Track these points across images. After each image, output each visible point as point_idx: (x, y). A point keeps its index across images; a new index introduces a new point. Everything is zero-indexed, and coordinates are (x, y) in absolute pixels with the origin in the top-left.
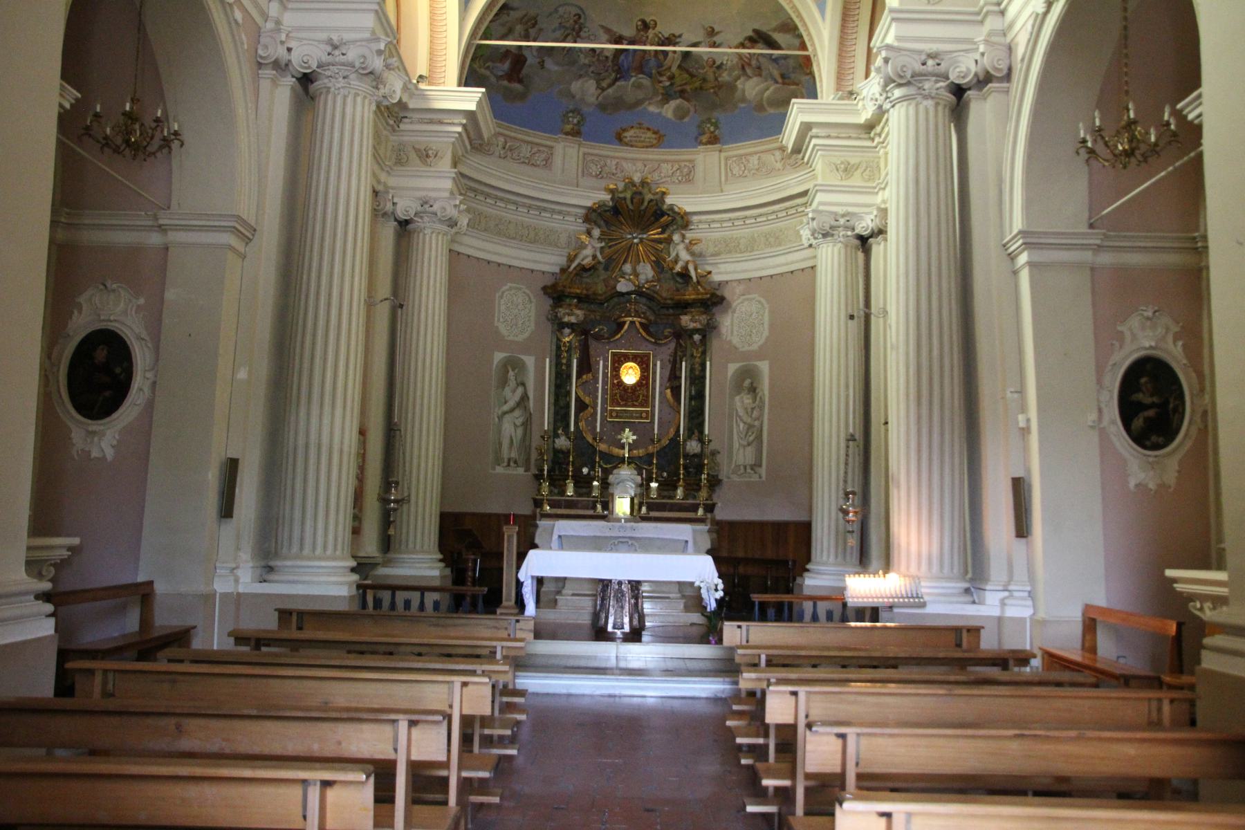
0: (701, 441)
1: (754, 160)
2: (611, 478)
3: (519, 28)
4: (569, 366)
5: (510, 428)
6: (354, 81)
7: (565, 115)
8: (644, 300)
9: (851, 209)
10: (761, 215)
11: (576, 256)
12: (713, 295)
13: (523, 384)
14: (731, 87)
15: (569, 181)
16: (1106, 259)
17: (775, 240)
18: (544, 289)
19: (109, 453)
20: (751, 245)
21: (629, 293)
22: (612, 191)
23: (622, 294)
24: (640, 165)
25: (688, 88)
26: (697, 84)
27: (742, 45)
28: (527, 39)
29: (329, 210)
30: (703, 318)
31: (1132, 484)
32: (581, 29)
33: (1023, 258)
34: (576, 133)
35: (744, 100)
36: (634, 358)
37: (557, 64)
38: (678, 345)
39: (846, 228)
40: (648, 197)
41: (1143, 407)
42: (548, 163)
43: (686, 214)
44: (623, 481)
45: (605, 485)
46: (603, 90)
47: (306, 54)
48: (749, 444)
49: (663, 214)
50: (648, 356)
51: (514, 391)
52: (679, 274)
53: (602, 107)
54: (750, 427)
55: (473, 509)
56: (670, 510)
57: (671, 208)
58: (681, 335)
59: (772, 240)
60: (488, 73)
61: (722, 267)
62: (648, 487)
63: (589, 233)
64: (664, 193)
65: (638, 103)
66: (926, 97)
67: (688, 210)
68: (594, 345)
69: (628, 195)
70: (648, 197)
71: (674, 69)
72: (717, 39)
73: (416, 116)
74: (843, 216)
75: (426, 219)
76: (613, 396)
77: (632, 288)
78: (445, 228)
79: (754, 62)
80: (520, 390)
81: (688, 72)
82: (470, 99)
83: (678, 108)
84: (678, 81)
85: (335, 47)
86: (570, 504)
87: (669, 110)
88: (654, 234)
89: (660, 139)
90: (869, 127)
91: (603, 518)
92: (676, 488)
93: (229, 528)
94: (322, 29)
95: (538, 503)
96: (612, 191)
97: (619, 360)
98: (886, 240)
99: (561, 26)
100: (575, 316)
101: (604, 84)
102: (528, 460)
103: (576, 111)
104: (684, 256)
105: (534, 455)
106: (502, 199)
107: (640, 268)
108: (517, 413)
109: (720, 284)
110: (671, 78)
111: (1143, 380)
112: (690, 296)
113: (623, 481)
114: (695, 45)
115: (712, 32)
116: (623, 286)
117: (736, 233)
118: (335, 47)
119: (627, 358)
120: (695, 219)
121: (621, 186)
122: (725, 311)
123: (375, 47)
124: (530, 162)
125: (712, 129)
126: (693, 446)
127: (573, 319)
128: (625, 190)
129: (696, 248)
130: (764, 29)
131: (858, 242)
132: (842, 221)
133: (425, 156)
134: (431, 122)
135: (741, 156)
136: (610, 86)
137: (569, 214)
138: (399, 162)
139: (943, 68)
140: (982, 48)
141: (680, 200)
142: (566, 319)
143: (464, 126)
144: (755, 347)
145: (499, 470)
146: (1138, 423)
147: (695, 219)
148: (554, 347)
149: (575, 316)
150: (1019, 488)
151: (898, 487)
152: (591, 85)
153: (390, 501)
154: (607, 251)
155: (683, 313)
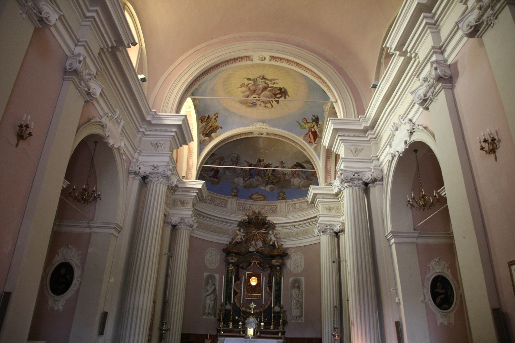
0: (280, 306)
1: (298, 205)
2: (246, 321)
3: (217, 161)
4: (232, 278)
5: (209, 301)
6: (161, 179)
7: (232, 190)
8: (259, 254)
9: (332, 223)
10: (300, 224)
11: (235, 238)
12: (284, 253)
13: (214, 285)
14: (289, 181)
15: (233, 212)
16: (420, 241)
17: (305, 233)
18: (223, 250)
19: (61, 308)
20: (297, 235)
21: (254, 252)
22: (248, 216)
23: (251, 252)
24: (258, 207)
25: (274, 181)
26: (277, 180)
27: (293, 167)
28: (220, 164)
29: (149, 222)
30: (280, 261)
31: (439, 324)
32: (238, 161)
33: (392, 241)
34: (236, 196)
35: (293, 185)
36: (255, 276)
37: (230, 172)
38: (271, 270)
39: (331, 229)
40: (261, 218)
41: (440, 294)
42: (225, 206)
43: (274, 224)
44: (251, 322)
45: (244, 324)
46: (245, 181)
47: (145, 170)
48: (298, 308)
49: (266, 224)
50: (260, 275)
51: (211, 287)
52: (271, 245)
53: (245, 187)
54: (298, 301)
55: (194, 332)
56: (268, 334)
57: (269, 221)
58: (272, 267)
59: (304, 233)
60: (206, 175)
61: (287, 243)
62: (260, 325)
63: (239, 230)
64: (266, 217)
65: (257, 186)
66: (355, 186)
67: (275, 222)
68: (241, 271)
69: (254, 217)
70: (261, 218)
71: (270, 175)
72: (284, 165)
73: (181, 189)
74: (329, 225)
75: (182, 225)
76: (247, 289)
77: (255, 250)
78: (189, 228)
79: (297, 173)
80: (213, 287)
81: (274, 176)
82: (199, 184)
83: (271, 188)
84: (271, 179)
85: (155, 168)
86: (231, 331)
87: (268, 188)
88: (263, 231)
89: (265, 198)
90: (337, 195)
91: (243, 337)
92: (271, 326)
93: (102, 339)
94: (151, 162)
95: (218, 331)
96: (248, 216)
97: (250, 276)
98: (344, 233)
99: (231, 161)
100: (234, 260)
101: (246, 180)
102: (215, 313)
103: (236, 188)
104: (274, 239)
105: (218, 311)
106: (209, 218)
107: (257, 243)
108: (212, 295)
109: (286, 249)
110: (269, 178)
111: (438, 284)
112: (276, 253)
113: (251, 322)
114: (277, 167)
115: (282, 163)
116: (251, 249)
117: (292, 231)
118: (155, 168)
120: (277, 225)
121: (251, 214)
122: (288, 259)
123: (168, 168)
124: (219, 205)
126: (277, 309)
127: (233, 261)
128: (252, 216)
129: (277, 236)
130: (300, 162)
131: (335, 234)
132: (329, 227)
133: (183, 203)
134: (186, 192)
135: (293, 204)
136: (248, 180)
137: (232, 223)
138: (174, 205)
139: (360, 176)
140: (373, 171)
141: (272, 219)
142: (231, 261)
143: (197, 193)
144: (299, 272)
145: (204, 317)
146: (438, 300)
147: (277, 225)
149: (234, 260)
150: (398, 325)
151: (354, 326)
152: (241, 180)
153: (163, 330)
154: (246, 236)
155: (273, 259)
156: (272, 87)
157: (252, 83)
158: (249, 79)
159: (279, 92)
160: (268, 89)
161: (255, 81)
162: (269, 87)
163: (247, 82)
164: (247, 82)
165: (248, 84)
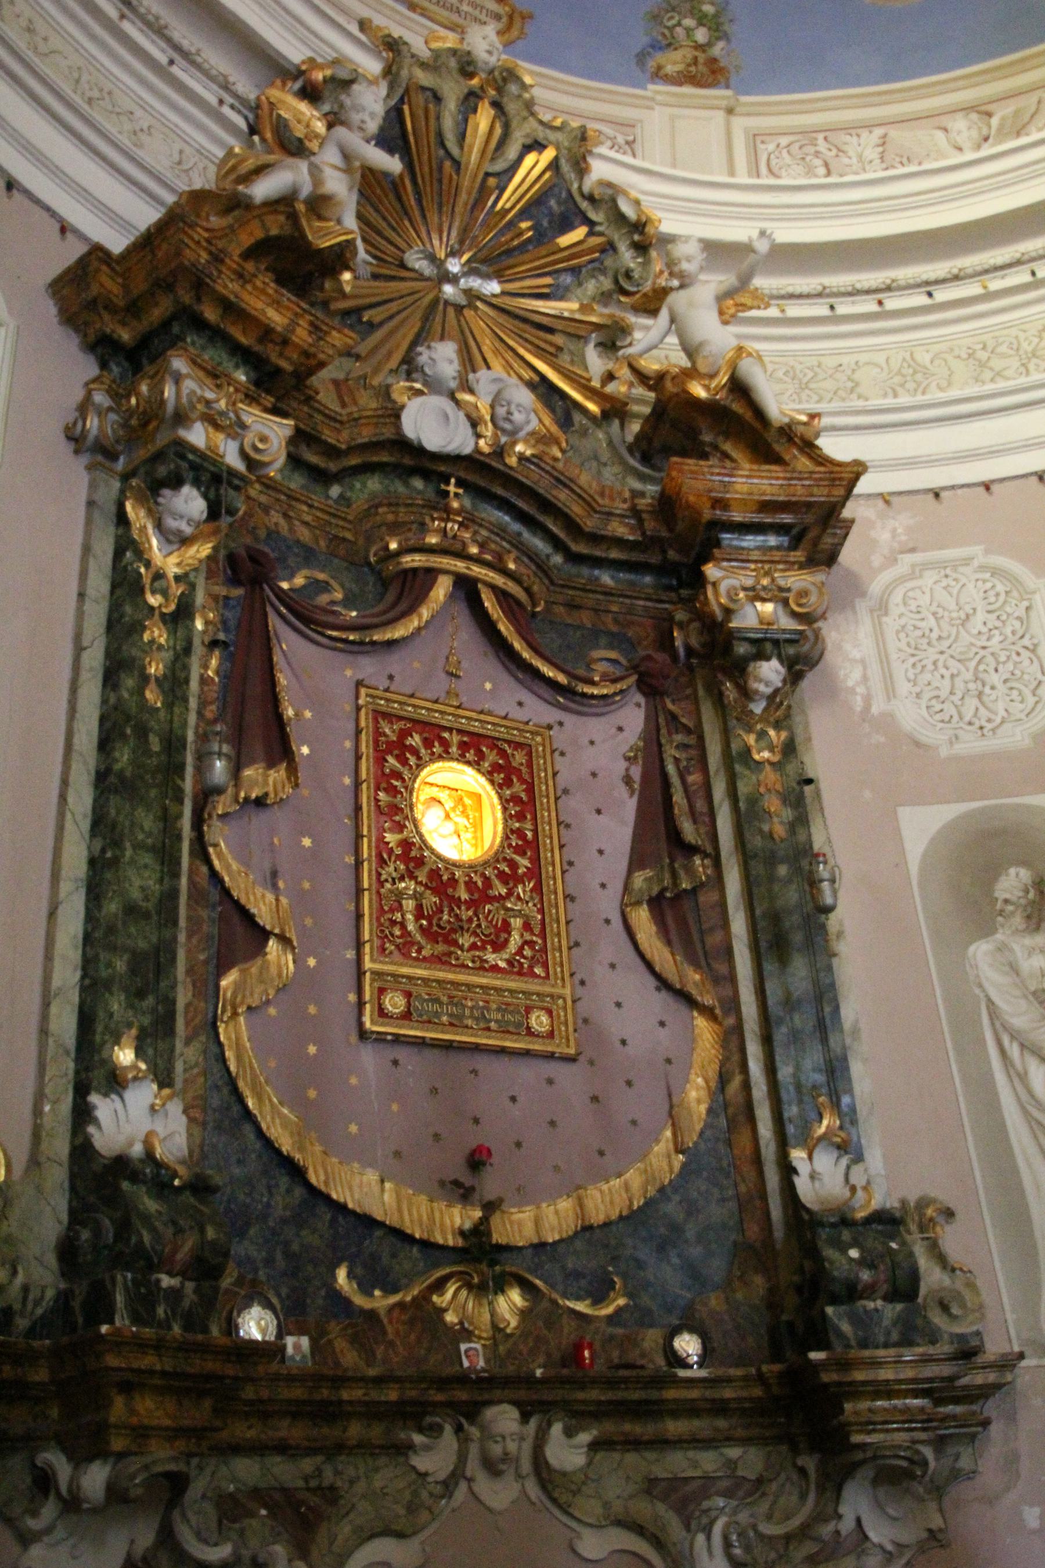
36: (473, 748)
57: (607, 198)
97: (402, 744)
119: (437, 740)
125: (701, 35)
135: (809, 134)
148: (100, 584)
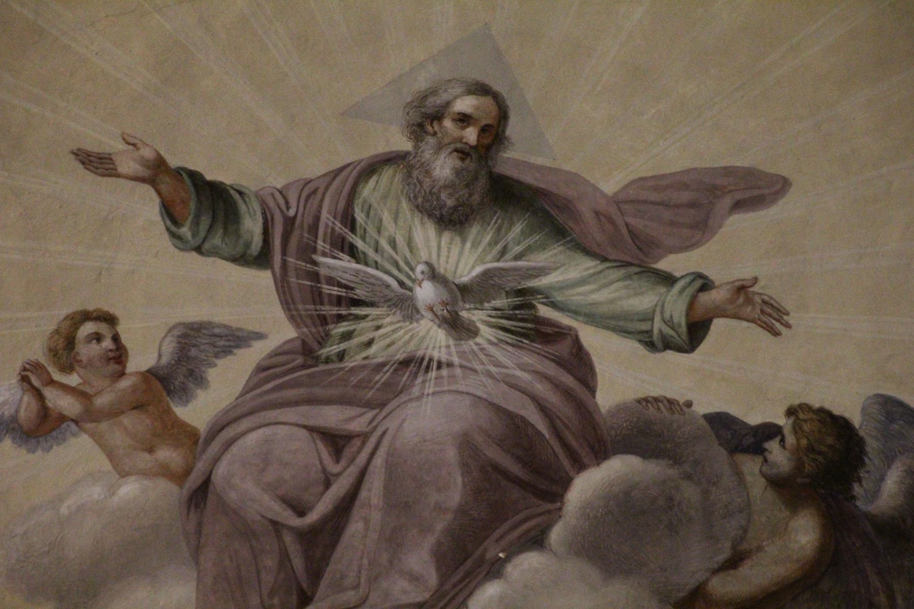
156: (650, 430)
157: (249, 301)
158: (202, 207)
159: (804, 534)
160: (587, 486)
161: (301, 241)
162: (596, 441)
163: (165, 287)
164: (165, 287)
165: (196, 347)
